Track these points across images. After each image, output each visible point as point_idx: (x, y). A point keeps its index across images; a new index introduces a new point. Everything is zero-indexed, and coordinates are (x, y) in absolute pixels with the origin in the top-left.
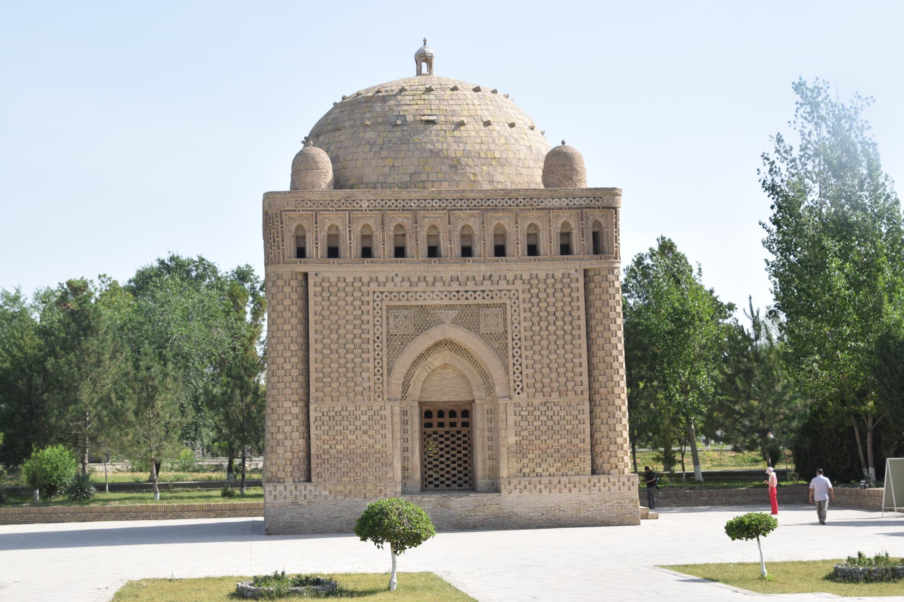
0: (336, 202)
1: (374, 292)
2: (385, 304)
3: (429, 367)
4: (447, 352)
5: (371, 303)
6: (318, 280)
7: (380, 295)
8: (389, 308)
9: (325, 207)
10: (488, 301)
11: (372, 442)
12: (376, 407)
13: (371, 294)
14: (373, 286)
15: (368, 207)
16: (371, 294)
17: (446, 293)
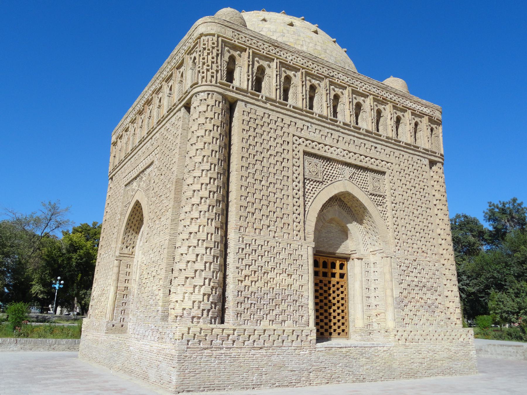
0: (267, 46)
1: (294, 136)
2: (302, 148)
3: (324, 217)
4: (337, 207)
5: (291, 143)
6: (248, 109)
7: (298, 139)
8: (306, 153)
9: (257, 47)
10: (375, 167)
11: (289, 281)
12: (294, 246)
13: (291, 135)
14: (292, 130)
15: (292, 60)
16: (291, 135)
17: (347, 152)
